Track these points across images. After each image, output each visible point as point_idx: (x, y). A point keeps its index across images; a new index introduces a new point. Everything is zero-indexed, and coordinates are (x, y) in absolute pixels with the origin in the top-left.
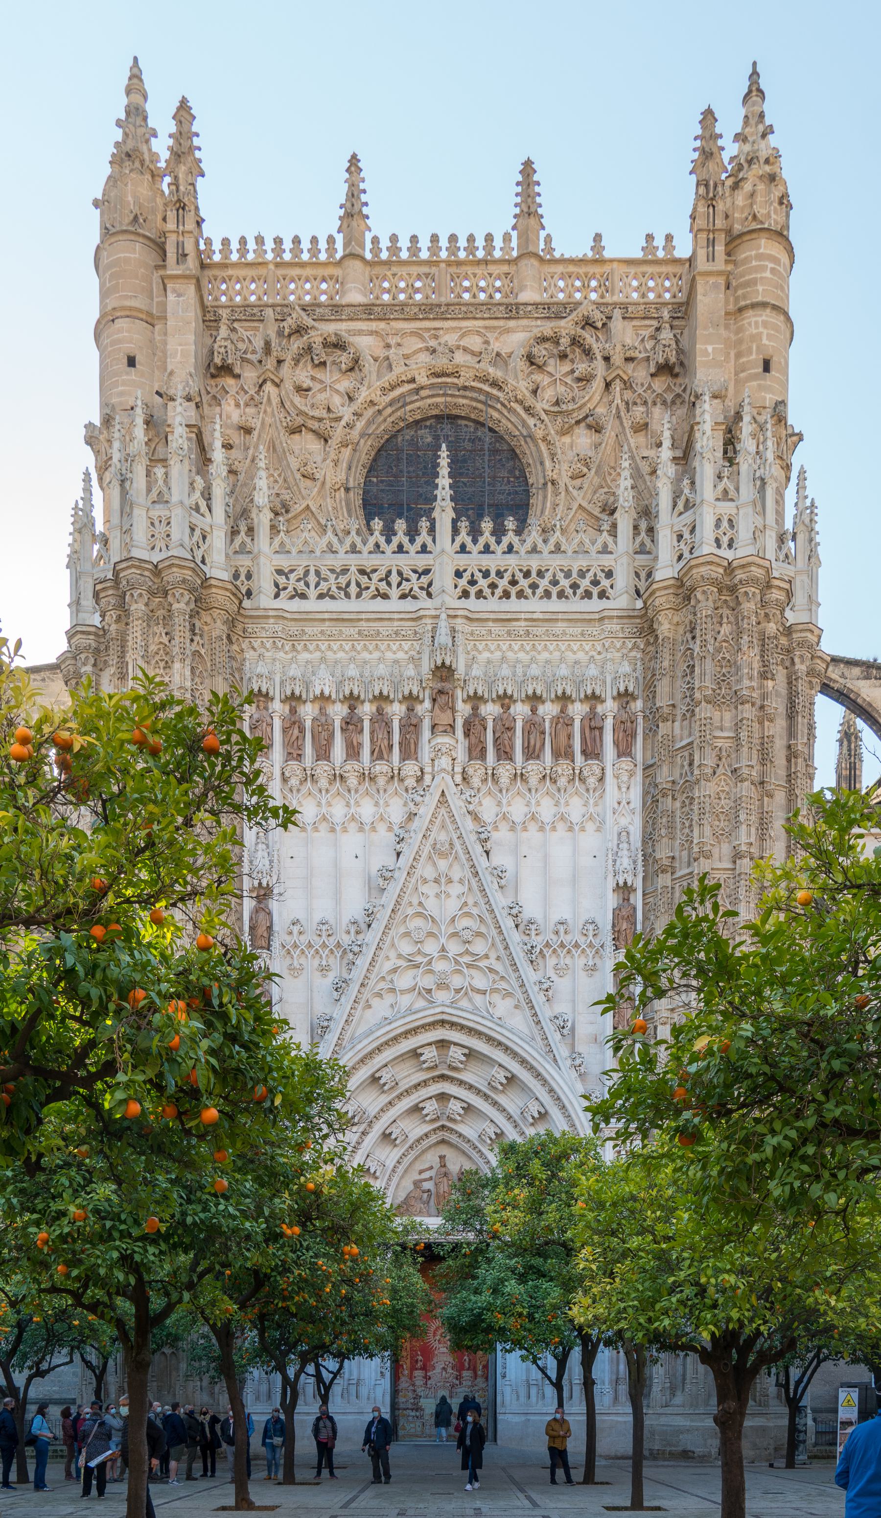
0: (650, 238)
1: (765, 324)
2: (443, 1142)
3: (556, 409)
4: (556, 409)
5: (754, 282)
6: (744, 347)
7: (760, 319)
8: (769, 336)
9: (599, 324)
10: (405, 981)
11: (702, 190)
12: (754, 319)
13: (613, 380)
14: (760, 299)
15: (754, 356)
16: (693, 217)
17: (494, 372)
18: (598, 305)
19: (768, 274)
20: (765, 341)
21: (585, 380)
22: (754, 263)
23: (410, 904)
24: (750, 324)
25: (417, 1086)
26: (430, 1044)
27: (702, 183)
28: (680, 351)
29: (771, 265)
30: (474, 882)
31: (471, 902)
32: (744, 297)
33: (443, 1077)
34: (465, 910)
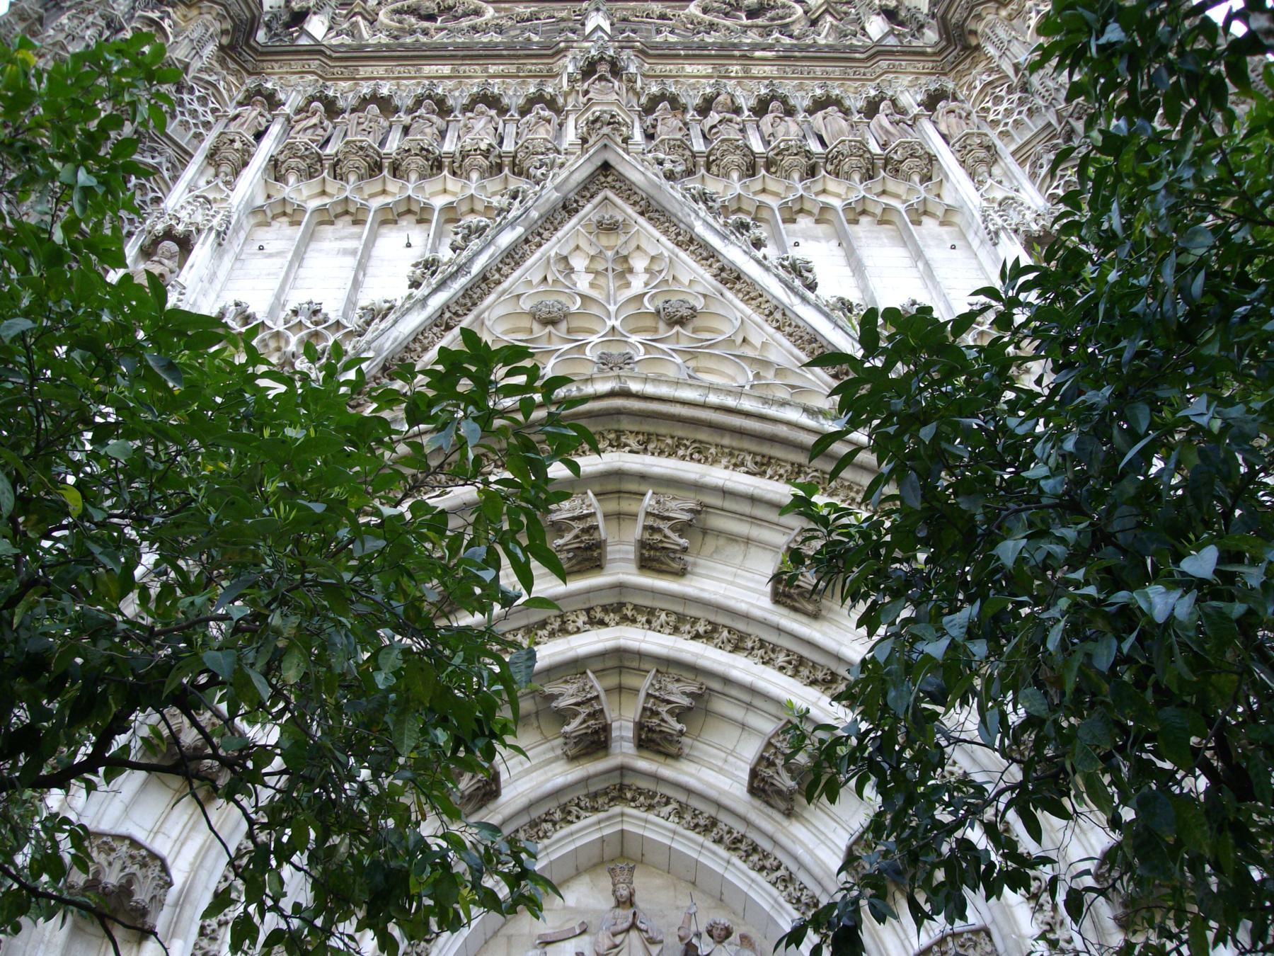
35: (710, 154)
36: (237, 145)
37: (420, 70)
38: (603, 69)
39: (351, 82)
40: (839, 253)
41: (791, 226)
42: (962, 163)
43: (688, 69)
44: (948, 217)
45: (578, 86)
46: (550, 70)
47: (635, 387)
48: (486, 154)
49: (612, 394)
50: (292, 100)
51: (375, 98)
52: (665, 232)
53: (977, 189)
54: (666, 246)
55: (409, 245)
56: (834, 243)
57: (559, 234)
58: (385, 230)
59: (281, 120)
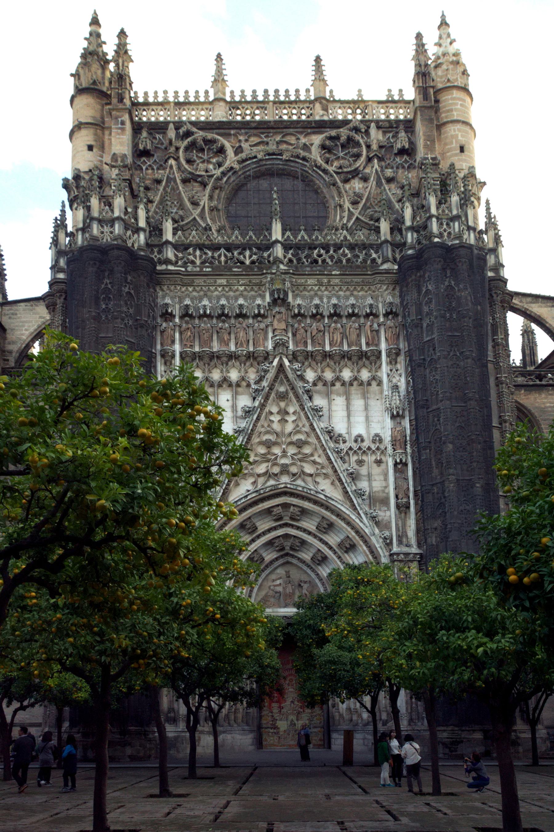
0: (390, 91)
1: (459, 130)
2: (288, 563)
3: (340, 171)
4: (340, 171)
5: (451, 110)
6: (447, 141)
7: (456, 128)
8: (462, 136)
9: (363, 130)
10: (261, 469)
11: (418, 69)
12: (452, 128)
13: (373, 156)
14: (455, 118)
15: (454, 145)
16: (414, 81)
17: (303, 153)
18: (362, 121)
19: (459, 107)
20: (460, 138)
21: (357, 156)
22: (450, 102)
23: (263, 426)
24: (450, 130)
25: (269, 530)
26: (278, 506)
27: (418, 65)
28: (411, 143)
29: (460, 103)
30: (302, 414)
31: (301, 425)
32: (446, 117)
33: (286, 525)
34: (298, 429)
35: (312, 352)
36: (170, 354)
37: (215, 282)
38: (279, 301)
39: (192, 288)
40: (345, 403)
41: (333, 388)
42: (388, 356)
43: (310, 281)
44: (380, 384)
45: (271, 308)
46: (261, 282)
47: (289, 486)
48: (245, 356)
49: (284, 487)
50: (177, 311)
51: (205, 315)
52: (298, 401)
53: (388, 376)
54: (298, 409)
55: (228, 400)
56: (345, 397)
57: (269, 402)
58: (219, 391)
59: (177, 328)
